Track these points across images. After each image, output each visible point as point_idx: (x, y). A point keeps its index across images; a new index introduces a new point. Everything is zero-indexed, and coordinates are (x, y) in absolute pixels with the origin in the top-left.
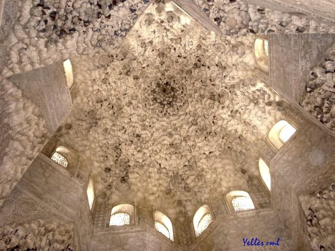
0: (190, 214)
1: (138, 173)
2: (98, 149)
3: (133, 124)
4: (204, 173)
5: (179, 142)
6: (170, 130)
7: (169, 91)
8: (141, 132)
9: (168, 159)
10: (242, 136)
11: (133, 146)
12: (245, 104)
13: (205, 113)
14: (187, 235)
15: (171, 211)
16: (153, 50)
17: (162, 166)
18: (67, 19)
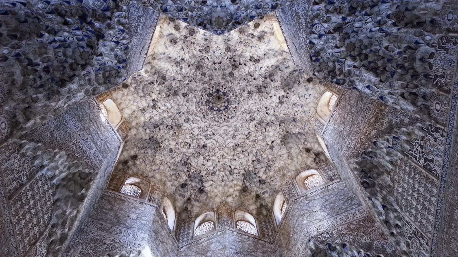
0: (270, 205)
1: (212, 181)
2: (168, 169)
3: (196, 137)
5: (243, 141)
9: (237, 159)
11: (201, 157)
14: (271, 226)
16: (189, 66)
17: (233, 167)
18: (65, 68)
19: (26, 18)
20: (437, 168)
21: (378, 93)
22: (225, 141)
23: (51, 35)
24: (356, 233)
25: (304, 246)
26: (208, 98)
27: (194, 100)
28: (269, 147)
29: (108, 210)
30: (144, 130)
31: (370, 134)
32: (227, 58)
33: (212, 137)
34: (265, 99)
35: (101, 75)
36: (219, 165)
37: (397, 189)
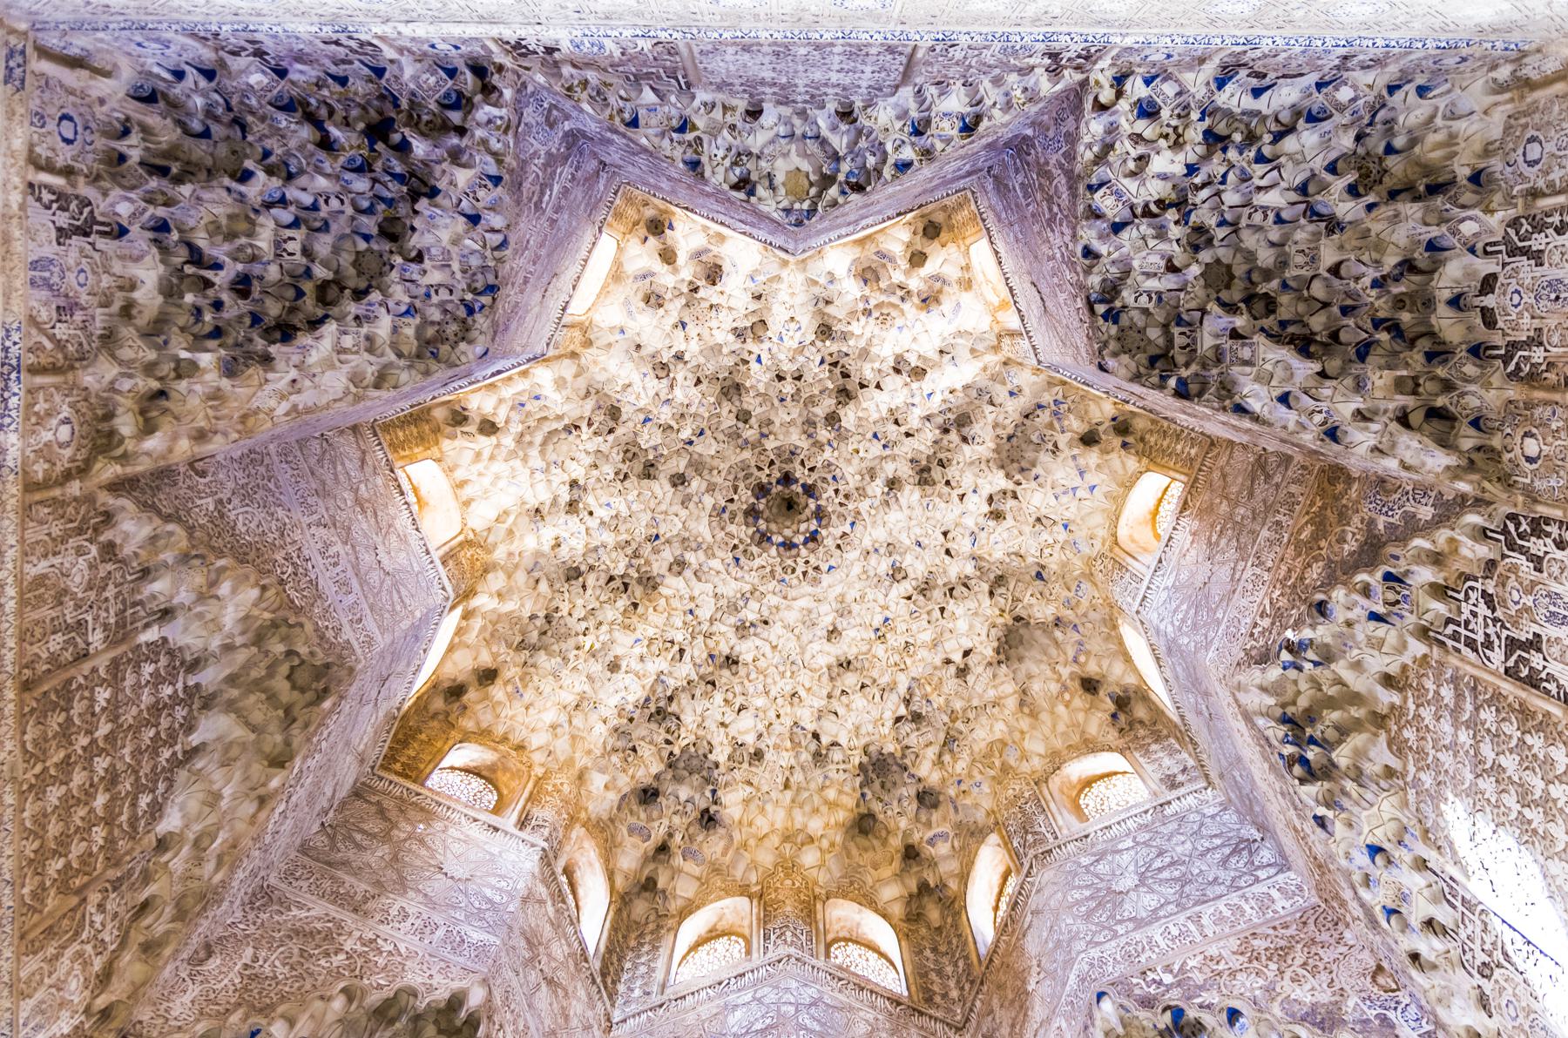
0: (953, 885)
3: (705, 627)
5: (864, 648)
11: (718, 697)
14: (956, 965)
16: (699, 381)
17: (825, 740)
20: (1554, 668)
21: (1318, 418)
24: (1273, 966)
25: (1081, 1019)
26: (753, 500)
27: (708, 501)
28: (952, 669)
29: (373, 836)
31: (1302, 579)
32: (822, 362)
34: (943, 505)
36: (777, 728)
37: (1417, 782)
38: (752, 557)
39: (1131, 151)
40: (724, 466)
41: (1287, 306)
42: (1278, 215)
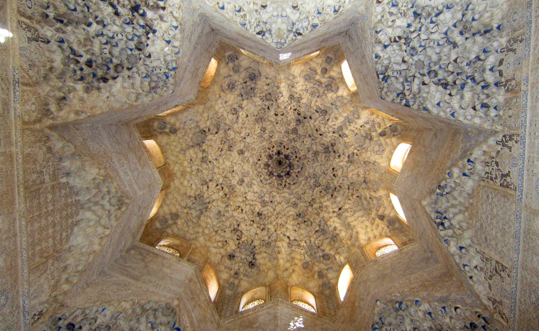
1: (266, 252)
2: (214, 233)
3: (251, 202)
4: (337, 232)
5: (305, 209)
6: (294, 200)
7: (284, 162)
8: (261, 210)
9: (297, 229)
10: (366, 178)
11: (255, 225)
12: (360, 144)
13: (324, 168)
15: (313, 284)
16: (247, 116)
17: (292, 238)
18: (109, 69)
19: (76, 5)
22: (284, 210)
23: (99, 26)
27: (251, 160)
30: (189, 185)
32: (291, 109)
33: (269, 204)
35: (147, 83)
38: (267, 180)
39: (389, 18)
40: (257, 148)
41: (441, 74)
42: (438, 43)
